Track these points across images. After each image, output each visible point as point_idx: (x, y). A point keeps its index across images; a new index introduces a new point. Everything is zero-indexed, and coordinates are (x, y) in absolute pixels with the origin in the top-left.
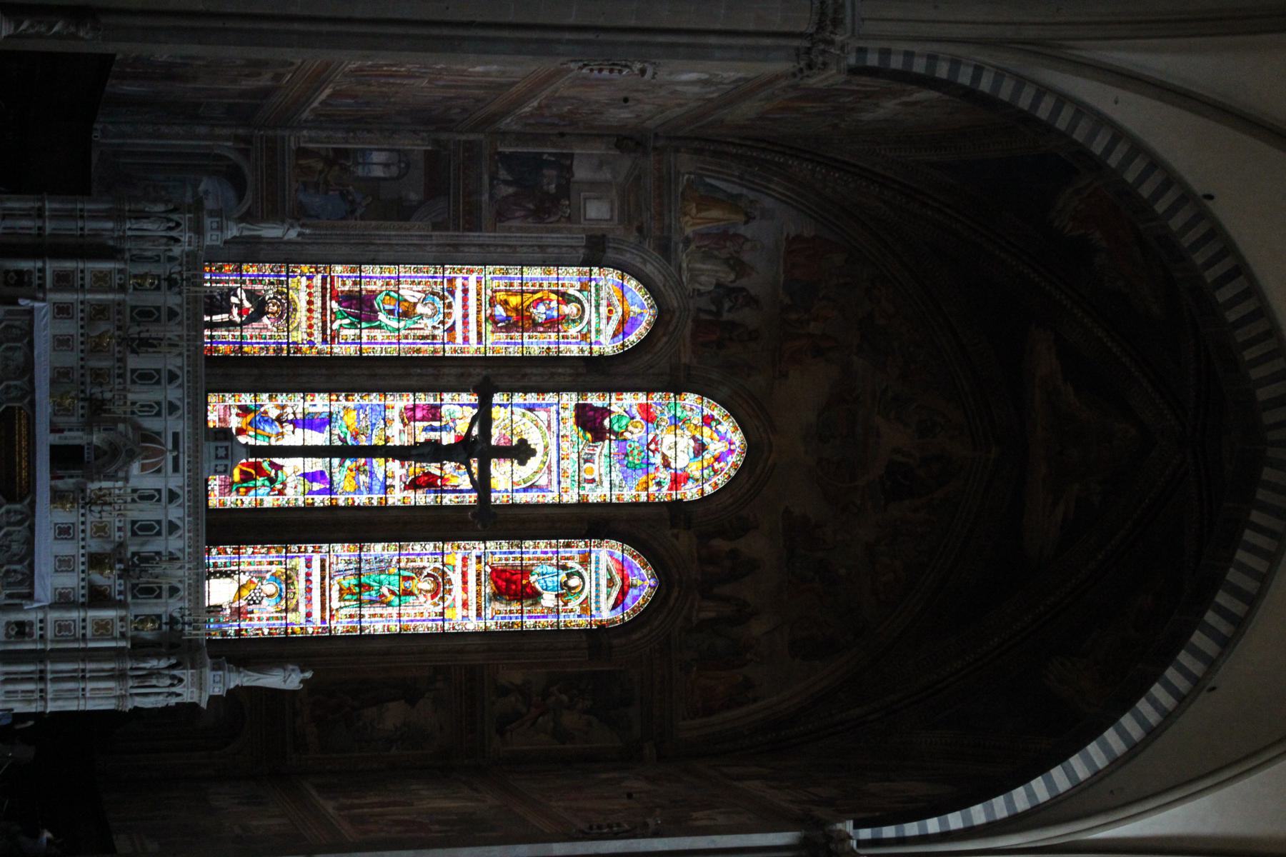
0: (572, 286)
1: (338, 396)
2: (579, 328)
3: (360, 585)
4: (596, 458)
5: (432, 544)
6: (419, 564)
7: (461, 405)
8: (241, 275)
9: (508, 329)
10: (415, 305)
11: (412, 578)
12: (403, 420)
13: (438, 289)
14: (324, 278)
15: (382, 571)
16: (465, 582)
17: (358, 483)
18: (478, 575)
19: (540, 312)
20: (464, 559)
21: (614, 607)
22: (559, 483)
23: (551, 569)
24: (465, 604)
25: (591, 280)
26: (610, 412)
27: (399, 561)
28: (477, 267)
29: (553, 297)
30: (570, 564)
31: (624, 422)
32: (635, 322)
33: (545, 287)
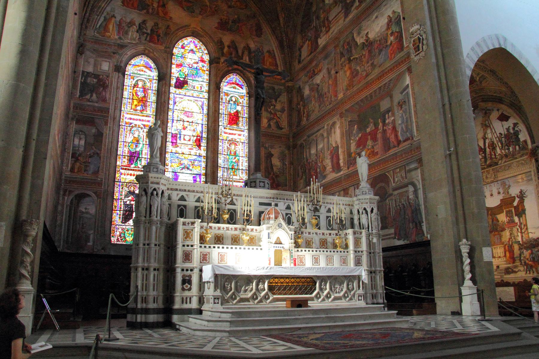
0: (132, 82)
1: (166, 169)
2: (148, 83)
3: (232, 169)
4: (193, 85)
5: (219, 143)
6: (226, 148)
7: (172, 127)
8: (119, 199)
9: (146, 106)
10: (134, 137)
11: (230, 151)
12: (176, 147)
13: (129, 128)
14: (122, 169)
15: (228, 161)
16: (232, 134)
17: (198, 165)
18: (230, 129)
19: (141, 94)
20: (225, 133)
21: (242, 88)
22: (201, 98)
23: (229, 106)
24: (240, 135)
25: (130, 75)
26: (178, 77)
27: (225, 155)
28: (122, 113)
29: (135, 89)
30: (228, 99)
31: (182, 74)
32: (147, 63)
33: (132, 91)
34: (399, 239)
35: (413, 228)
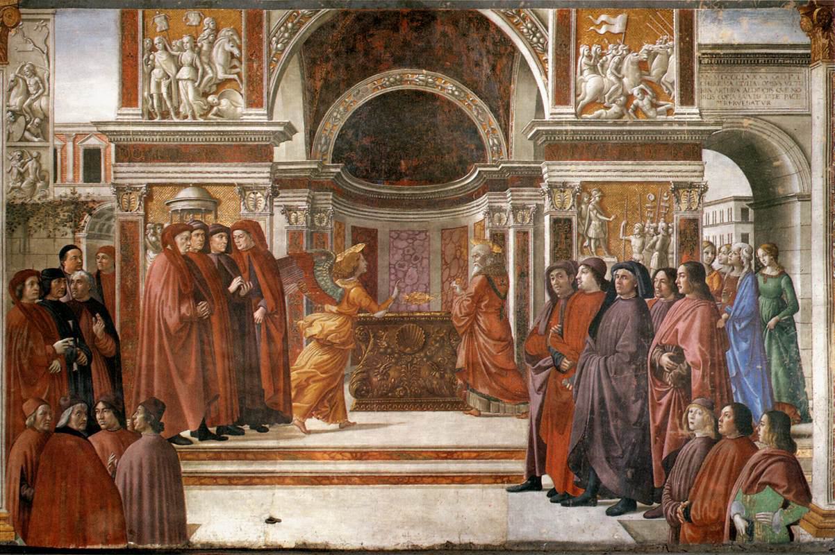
34: (559, 497)
35: (710, 443)
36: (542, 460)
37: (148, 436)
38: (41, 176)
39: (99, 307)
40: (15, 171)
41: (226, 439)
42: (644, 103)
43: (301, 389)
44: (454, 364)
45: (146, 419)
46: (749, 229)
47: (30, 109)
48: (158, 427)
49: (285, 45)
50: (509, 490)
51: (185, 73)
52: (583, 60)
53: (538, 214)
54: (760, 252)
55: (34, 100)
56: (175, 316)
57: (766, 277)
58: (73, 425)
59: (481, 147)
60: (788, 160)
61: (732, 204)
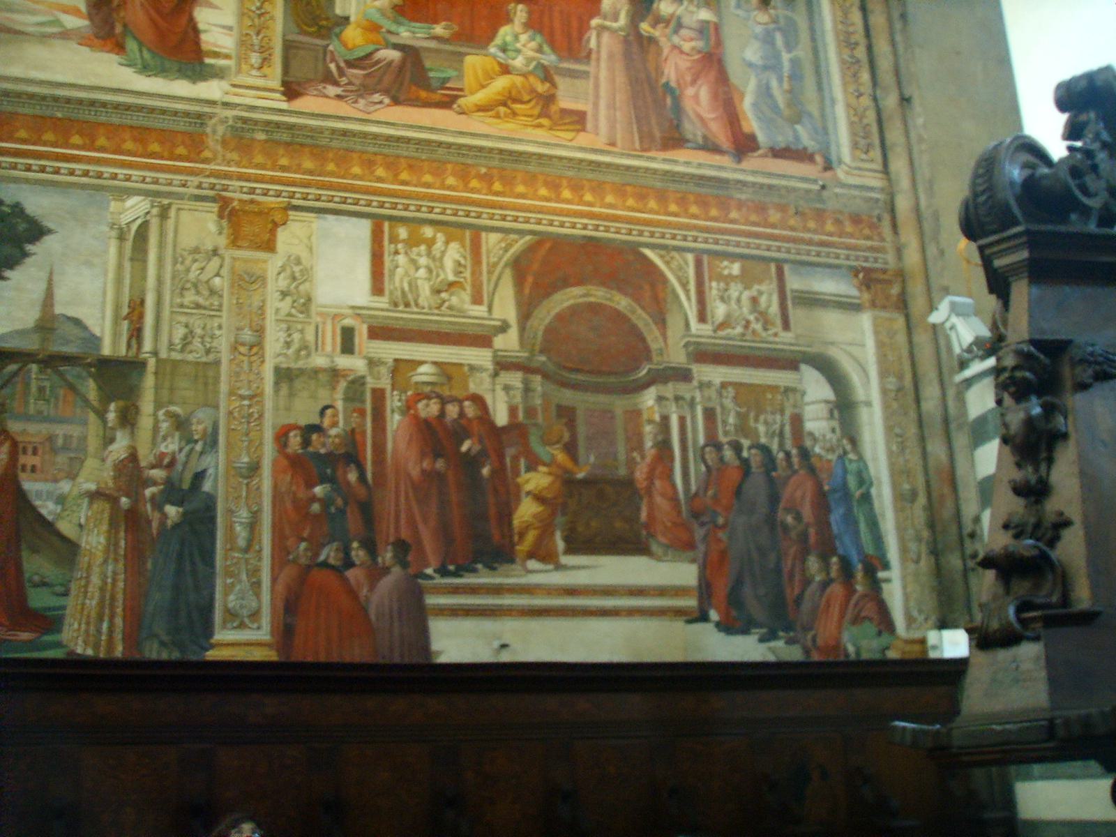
34: (727, 627)
35: (825, 585)
36: (710, 595)
37: (397, 571)
38: (304, 347)
39: (352, 457)
40: (282, 340)
41: (461, 576)
42: (758, 327)
43: (522, 535)
44: (638, 518)
45: (395, 556)
46: (835, 424)
47: (297, 290)
48: (405, 565)
49: (500, 259)
50: (689, 622)
51: (422, 273)
52: (714, 292)
53: (692, 404)
54: (845, 442)
55: (300, 284)
56: (418, 469)
57: (851, 461)
58: (332, 561)
59: (647, 349)
60: (855, 378)
61: (823, 405)
